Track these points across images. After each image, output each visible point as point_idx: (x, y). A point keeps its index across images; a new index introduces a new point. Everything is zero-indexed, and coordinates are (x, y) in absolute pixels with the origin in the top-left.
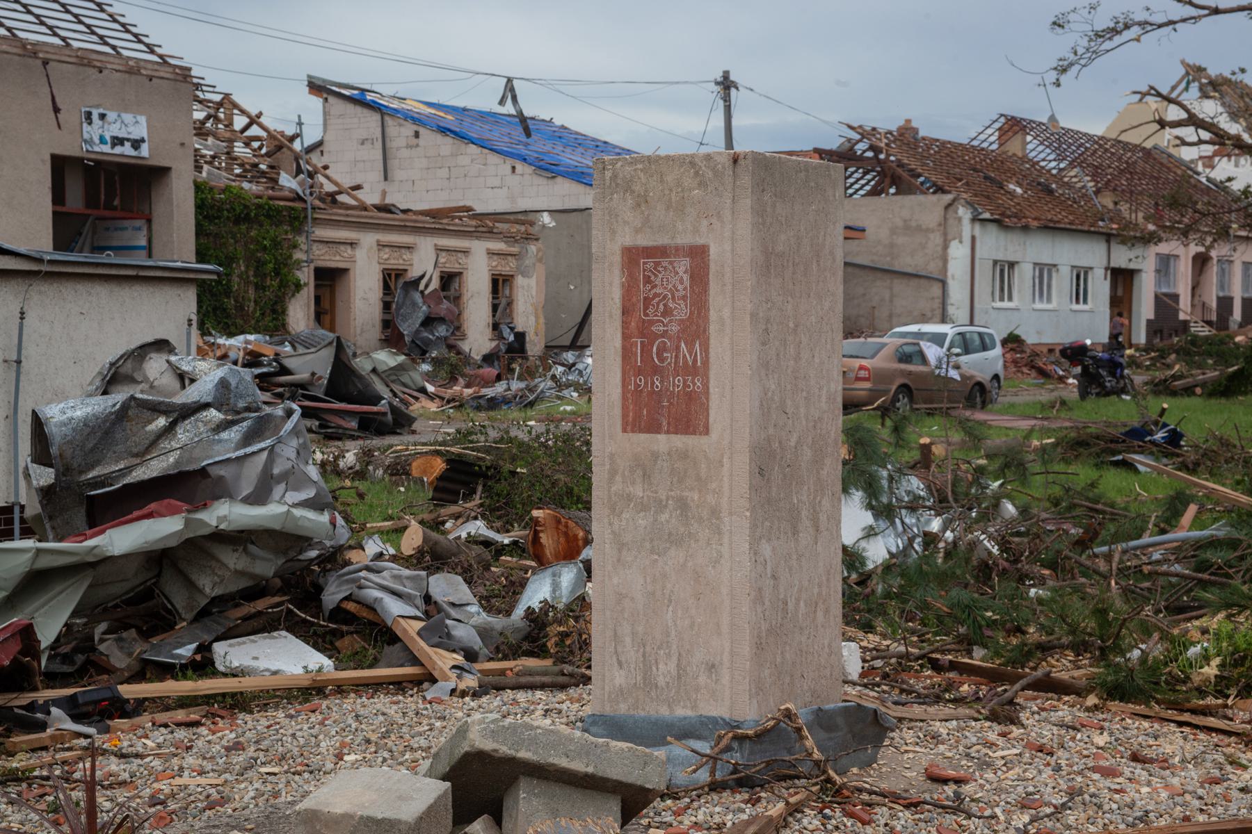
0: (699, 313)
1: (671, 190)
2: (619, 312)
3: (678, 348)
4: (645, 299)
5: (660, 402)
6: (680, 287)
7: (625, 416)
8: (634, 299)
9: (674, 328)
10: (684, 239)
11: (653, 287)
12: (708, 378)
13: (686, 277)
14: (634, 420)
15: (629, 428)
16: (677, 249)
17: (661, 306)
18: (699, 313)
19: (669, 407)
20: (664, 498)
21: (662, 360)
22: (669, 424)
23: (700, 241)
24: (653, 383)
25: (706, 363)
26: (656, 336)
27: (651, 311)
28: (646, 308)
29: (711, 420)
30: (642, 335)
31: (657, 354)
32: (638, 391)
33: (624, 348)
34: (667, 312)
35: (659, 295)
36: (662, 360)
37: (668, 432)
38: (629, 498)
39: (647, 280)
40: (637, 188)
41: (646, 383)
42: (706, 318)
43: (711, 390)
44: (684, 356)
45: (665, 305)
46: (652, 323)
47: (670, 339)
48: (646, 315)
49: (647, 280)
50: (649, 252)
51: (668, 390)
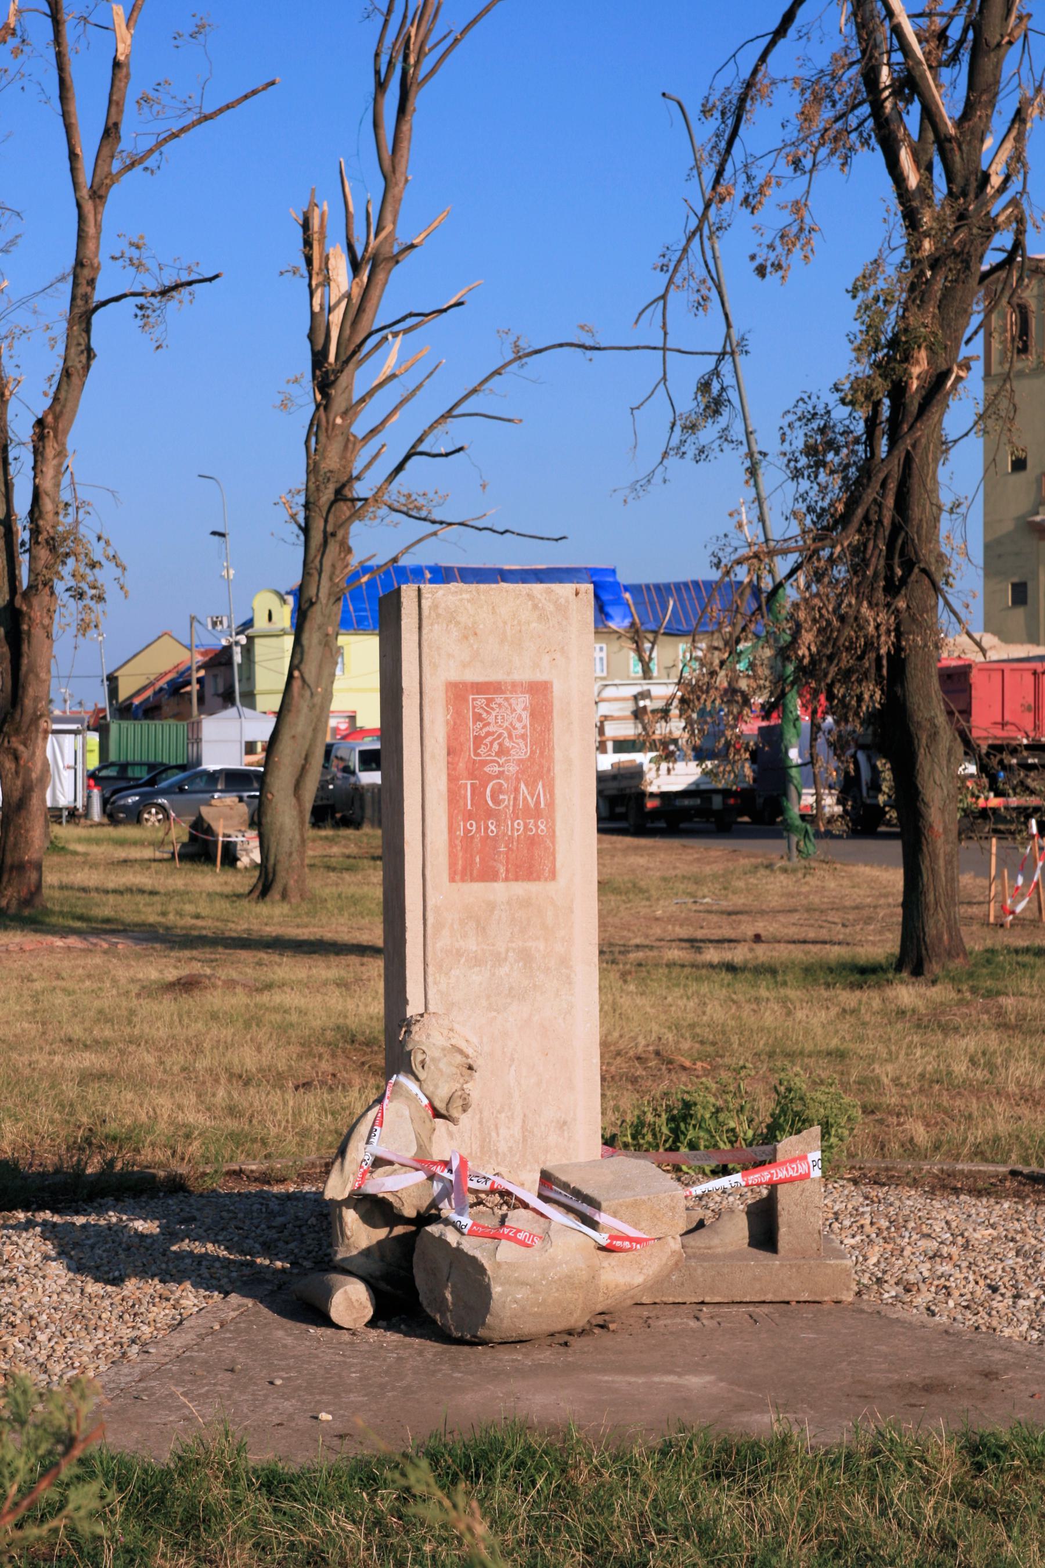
0: (542, 753)
1: (505, 623)
2: (445, 752)
3: (517, 790)
4: (475, 737)
5: (495, 848)
6: (518, 725)
7: (452, 865)
8: (462, 739)
9: (512, 769)
10: (524, 674)
11: (485, 725)
12: (554, 821)
13: (525, 715)
14: (464, 869)
15: (458, 877)
16: (514, 685)
17: (496, 746)
18: (542, 753)
19: (507, 853)
20: (503, 950)
21: (497, 802)
22: (507, 871)
23: (539, 677)
24: (487, 828)
25: (551, 805)
26: (491, 778)
27: (482, 750)
28: (477, 747)
29: (558, 865)
30: (472, 776)
31: (492, 796)
32: (468, 838)
33: (450, 791)
34: (502, 751)
35: (493, 733)
36: (497, 802)
37: (506, 879)
38: (459, 954)
39: (478, 718)
40: (463, 619)
41: (478, 828)
42: (551, 759)
43: (558, 833)
44: (525, 799)
45: (500, 744)
46: (484, 763)
47: (507, 779)
48: (479, 755)
49: (478, 718)
50: (480, 688)
51: (505, 834)
